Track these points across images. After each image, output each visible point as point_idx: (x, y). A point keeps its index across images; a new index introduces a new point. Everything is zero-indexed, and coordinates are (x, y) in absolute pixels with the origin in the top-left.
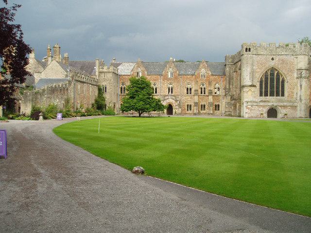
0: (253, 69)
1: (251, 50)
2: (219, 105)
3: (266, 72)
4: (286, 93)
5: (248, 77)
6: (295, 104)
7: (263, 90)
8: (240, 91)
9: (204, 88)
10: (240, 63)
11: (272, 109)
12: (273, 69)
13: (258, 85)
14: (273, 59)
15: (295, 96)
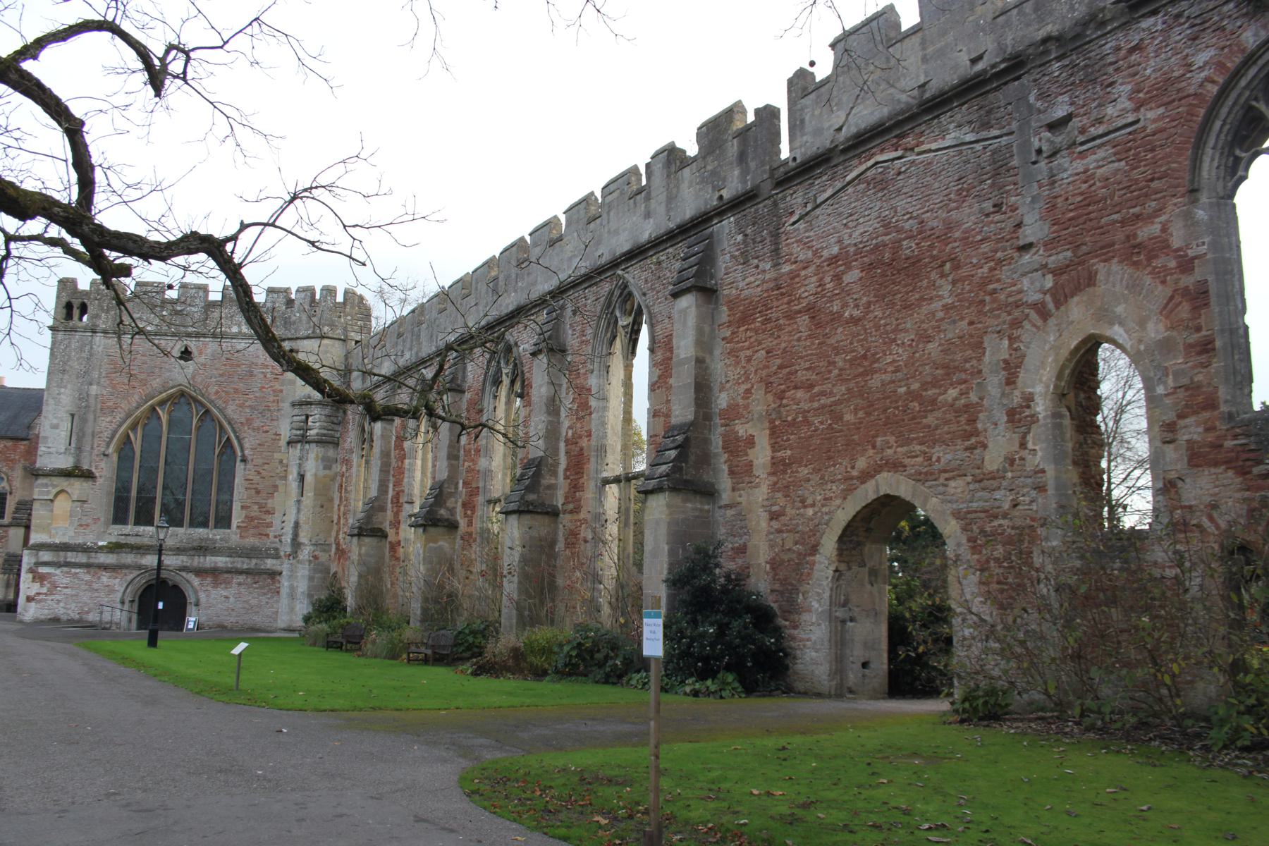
0: (83, 397)
3: (153, 409)
4: (237, 517)
5: (63, 433)
6: (270, 563)
12: (182, 397)
13: (105, 470)
14: (186, 355)
15: (276, 521)
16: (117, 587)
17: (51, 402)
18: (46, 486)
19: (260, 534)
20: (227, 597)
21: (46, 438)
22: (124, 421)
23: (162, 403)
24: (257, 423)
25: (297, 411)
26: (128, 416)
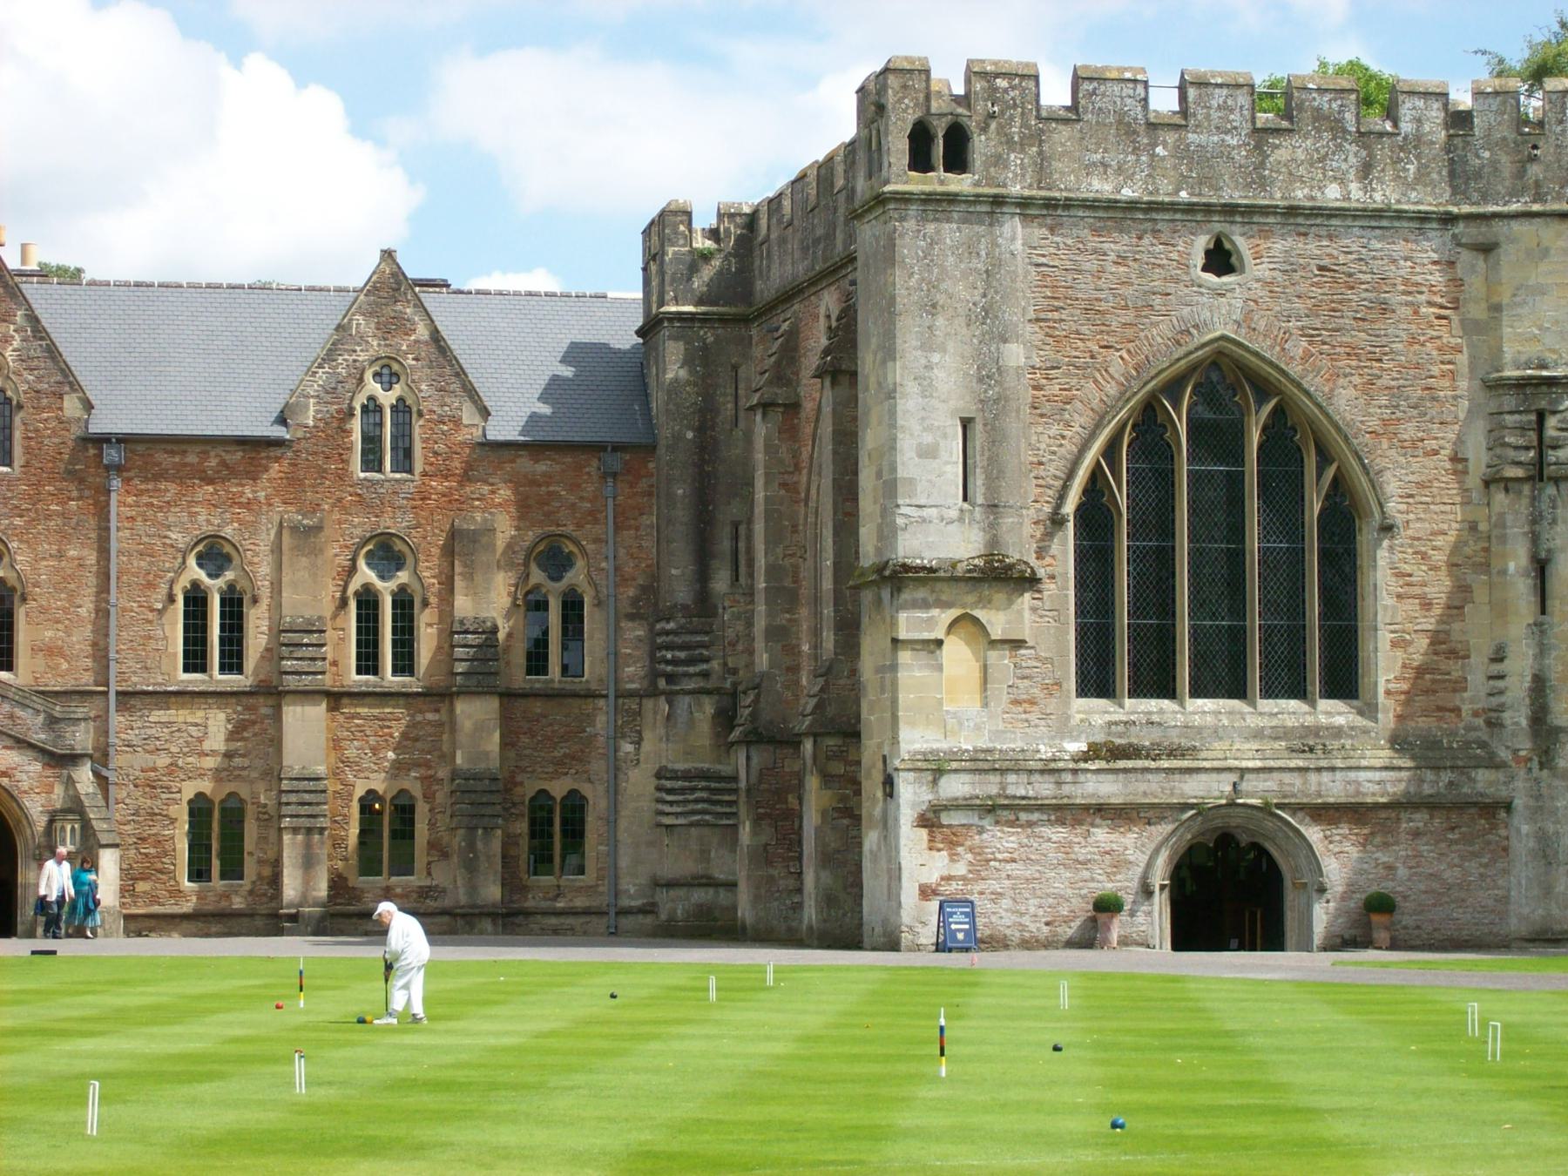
1: (981, 146)
2: (575, 807)
6: (1484, 781)
7: (1123, 618)
8: (849, 630)
9: (404, 605)
10: (829, 302)
11: (1226, 839)
14: (1220, 260)
15: (1477, 682)
16: (1132, 855)
17: (911, 387)
18: (925, 605)
19: (1440, 709)
20: (1390, 868)
21: (911, 481)
22: (1093, 436)
23: (1173, 388)
24: (1409, 431)
25: (1509, 401)
26: (1098, 427)
